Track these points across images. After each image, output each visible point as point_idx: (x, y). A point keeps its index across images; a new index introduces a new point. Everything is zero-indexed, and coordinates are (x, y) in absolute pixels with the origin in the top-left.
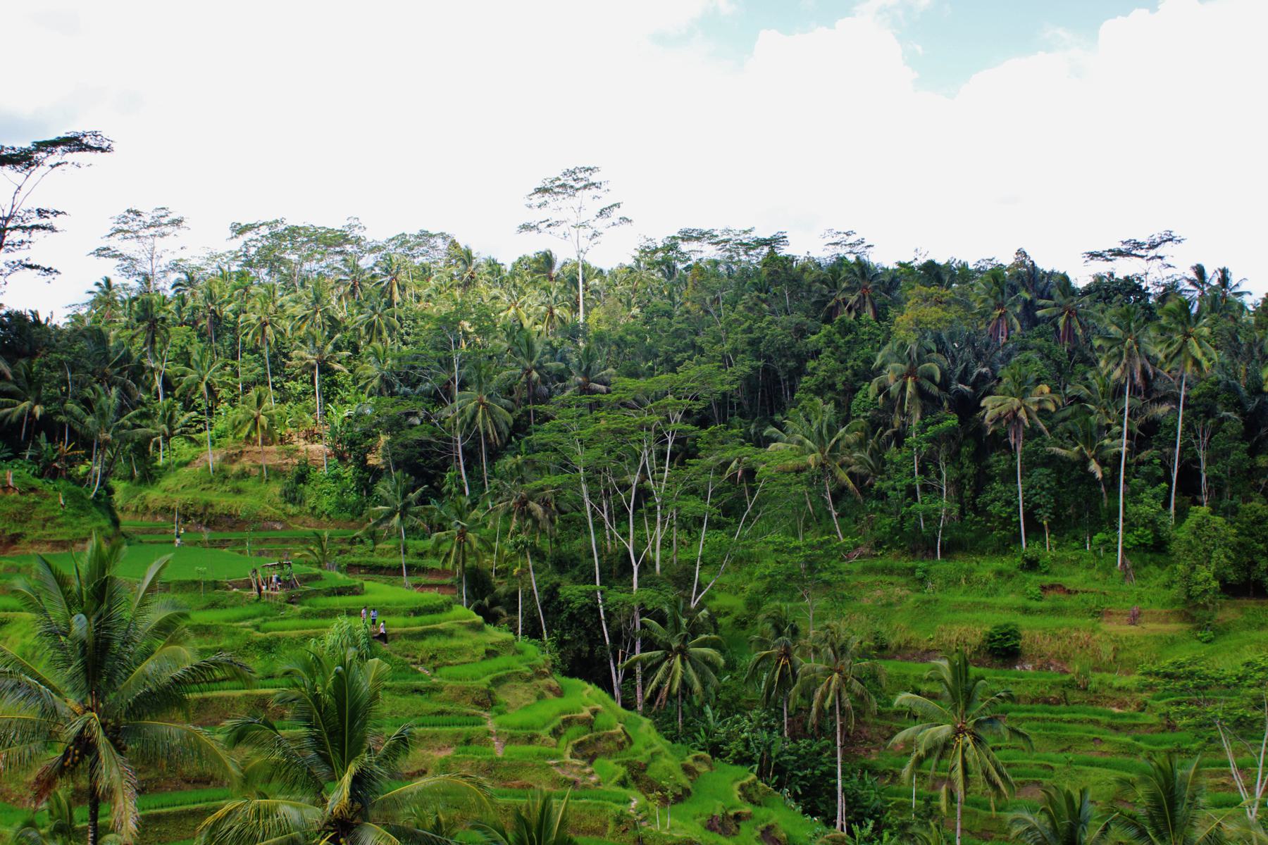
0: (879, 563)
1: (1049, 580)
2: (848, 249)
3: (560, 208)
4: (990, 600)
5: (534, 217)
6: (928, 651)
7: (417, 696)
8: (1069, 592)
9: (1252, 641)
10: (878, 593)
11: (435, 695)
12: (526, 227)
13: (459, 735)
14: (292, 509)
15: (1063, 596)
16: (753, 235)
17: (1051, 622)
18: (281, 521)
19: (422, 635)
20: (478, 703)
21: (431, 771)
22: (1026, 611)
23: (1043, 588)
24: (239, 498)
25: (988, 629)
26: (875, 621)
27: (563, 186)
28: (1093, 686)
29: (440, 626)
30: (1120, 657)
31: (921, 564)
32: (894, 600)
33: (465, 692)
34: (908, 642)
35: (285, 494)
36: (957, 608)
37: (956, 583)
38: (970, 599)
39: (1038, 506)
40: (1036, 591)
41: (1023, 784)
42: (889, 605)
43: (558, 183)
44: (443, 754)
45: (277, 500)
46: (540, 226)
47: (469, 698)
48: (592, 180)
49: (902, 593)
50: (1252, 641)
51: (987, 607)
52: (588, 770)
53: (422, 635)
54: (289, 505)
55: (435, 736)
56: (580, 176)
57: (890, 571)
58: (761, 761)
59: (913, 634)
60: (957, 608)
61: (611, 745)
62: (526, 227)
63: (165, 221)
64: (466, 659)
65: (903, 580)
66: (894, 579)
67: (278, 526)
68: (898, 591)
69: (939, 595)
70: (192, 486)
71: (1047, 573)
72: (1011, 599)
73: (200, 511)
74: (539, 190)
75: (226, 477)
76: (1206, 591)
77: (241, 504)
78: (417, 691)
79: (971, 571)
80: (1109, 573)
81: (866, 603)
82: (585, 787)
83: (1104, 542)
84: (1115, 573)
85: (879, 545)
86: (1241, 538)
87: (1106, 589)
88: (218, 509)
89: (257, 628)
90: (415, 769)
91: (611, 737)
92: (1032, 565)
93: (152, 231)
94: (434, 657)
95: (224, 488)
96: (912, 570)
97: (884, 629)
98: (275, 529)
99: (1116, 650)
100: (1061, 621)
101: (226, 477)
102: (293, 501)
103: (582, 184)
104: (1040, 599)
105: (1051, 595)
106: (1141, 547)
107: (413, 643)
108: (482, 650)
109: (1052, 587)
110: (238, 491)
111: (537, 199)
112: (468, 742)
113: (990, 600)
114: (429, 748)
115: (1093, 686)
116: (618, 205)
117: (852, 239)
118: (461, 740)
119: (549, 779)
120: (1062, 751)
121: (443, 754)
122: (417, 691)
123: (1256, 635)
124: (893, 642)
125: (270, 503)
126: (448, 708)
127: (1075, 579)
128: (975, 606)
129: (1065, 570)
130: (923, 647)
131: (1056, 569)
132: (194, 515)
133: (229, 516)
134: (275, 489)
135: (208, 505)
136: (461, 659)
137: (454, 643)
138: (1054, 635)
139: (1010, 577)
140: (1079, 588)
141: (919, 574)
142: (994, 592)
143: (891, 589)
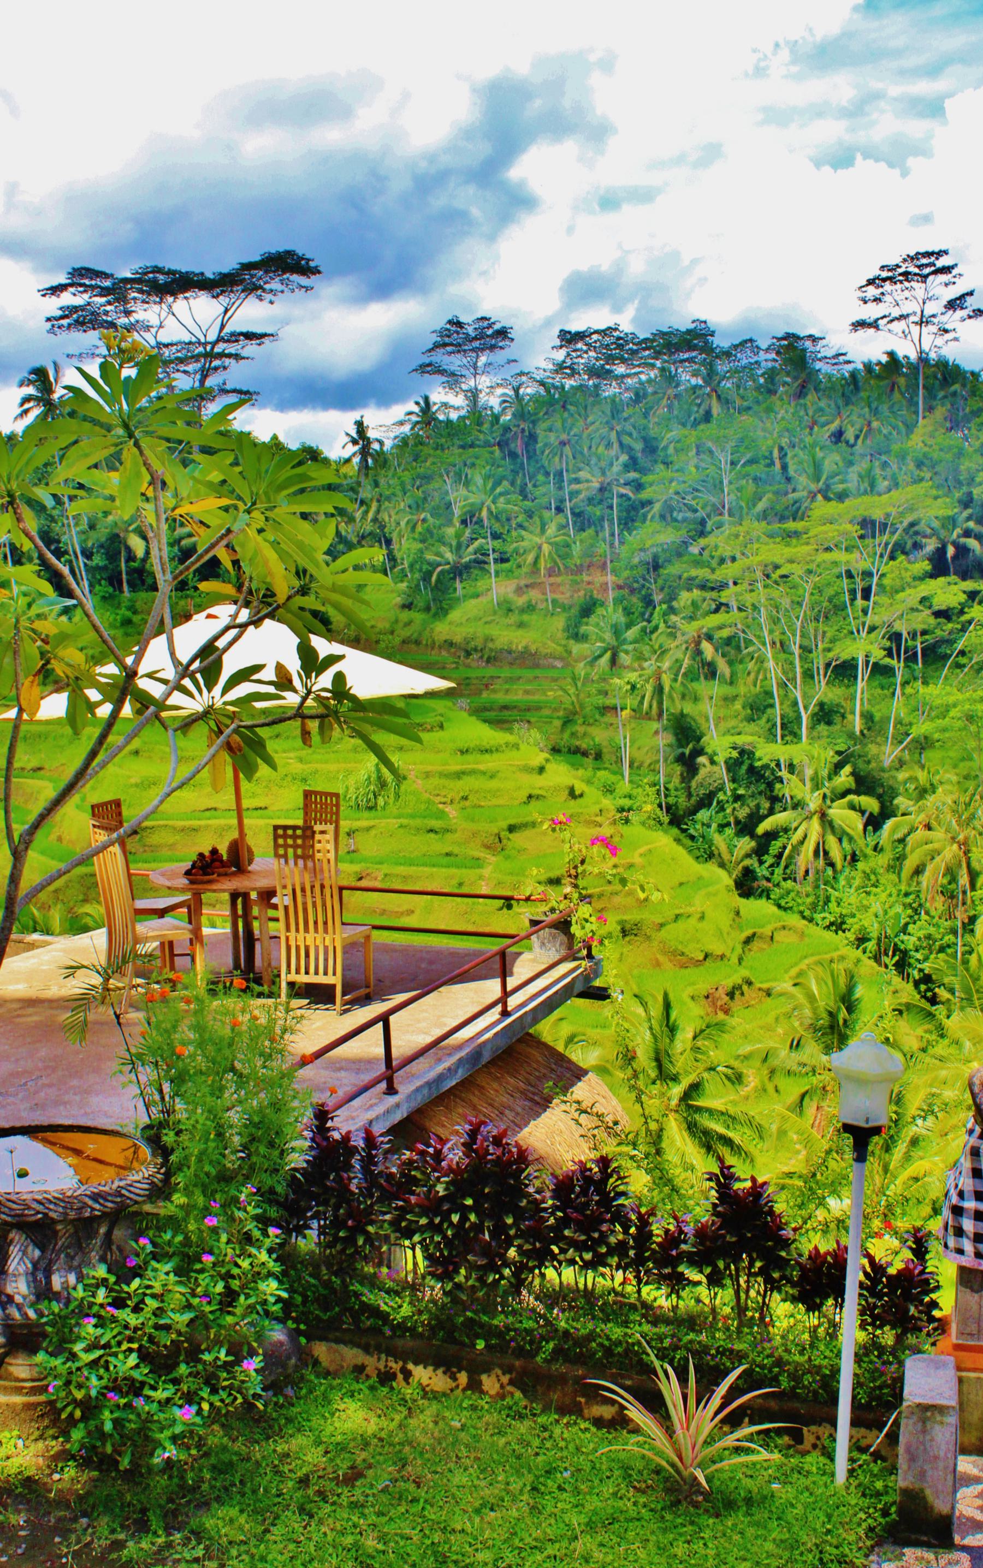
3: (905, 299)
5: (871, 312)
7: (432, 835)
11: (448, 836)
12: (860, 325)
13: (452, 877)
18: (561, 659)
19: (459, 775)
20: (487, 847)
21: (418, 912)
24: (520, 632)
29: (482, 767)
33: (474, 834)
35: (567, 629)
43: (900, 270)
45: (560, 635)
53: (459, 775)
54: (572, 642)
56: (924, 261)
58: (879, 939)
62: (860, 325)
63: (490, 332)
64: (501, 802)
67: (559, 664)
74: (871, 282)
75: (510, 610)
77: (519, 639)
88: (498, 644)
89: (301, 760)
93: (476, 344)
94: (465, 798)
98: (554, 667)
101: (510, 610)
108: (523, 795)
110: (521, 625)
111: (872, 291)
125: (552, 638)
126: (456, 850)
132: (476, 650)
134: (559, 623)
137: (493, 784)
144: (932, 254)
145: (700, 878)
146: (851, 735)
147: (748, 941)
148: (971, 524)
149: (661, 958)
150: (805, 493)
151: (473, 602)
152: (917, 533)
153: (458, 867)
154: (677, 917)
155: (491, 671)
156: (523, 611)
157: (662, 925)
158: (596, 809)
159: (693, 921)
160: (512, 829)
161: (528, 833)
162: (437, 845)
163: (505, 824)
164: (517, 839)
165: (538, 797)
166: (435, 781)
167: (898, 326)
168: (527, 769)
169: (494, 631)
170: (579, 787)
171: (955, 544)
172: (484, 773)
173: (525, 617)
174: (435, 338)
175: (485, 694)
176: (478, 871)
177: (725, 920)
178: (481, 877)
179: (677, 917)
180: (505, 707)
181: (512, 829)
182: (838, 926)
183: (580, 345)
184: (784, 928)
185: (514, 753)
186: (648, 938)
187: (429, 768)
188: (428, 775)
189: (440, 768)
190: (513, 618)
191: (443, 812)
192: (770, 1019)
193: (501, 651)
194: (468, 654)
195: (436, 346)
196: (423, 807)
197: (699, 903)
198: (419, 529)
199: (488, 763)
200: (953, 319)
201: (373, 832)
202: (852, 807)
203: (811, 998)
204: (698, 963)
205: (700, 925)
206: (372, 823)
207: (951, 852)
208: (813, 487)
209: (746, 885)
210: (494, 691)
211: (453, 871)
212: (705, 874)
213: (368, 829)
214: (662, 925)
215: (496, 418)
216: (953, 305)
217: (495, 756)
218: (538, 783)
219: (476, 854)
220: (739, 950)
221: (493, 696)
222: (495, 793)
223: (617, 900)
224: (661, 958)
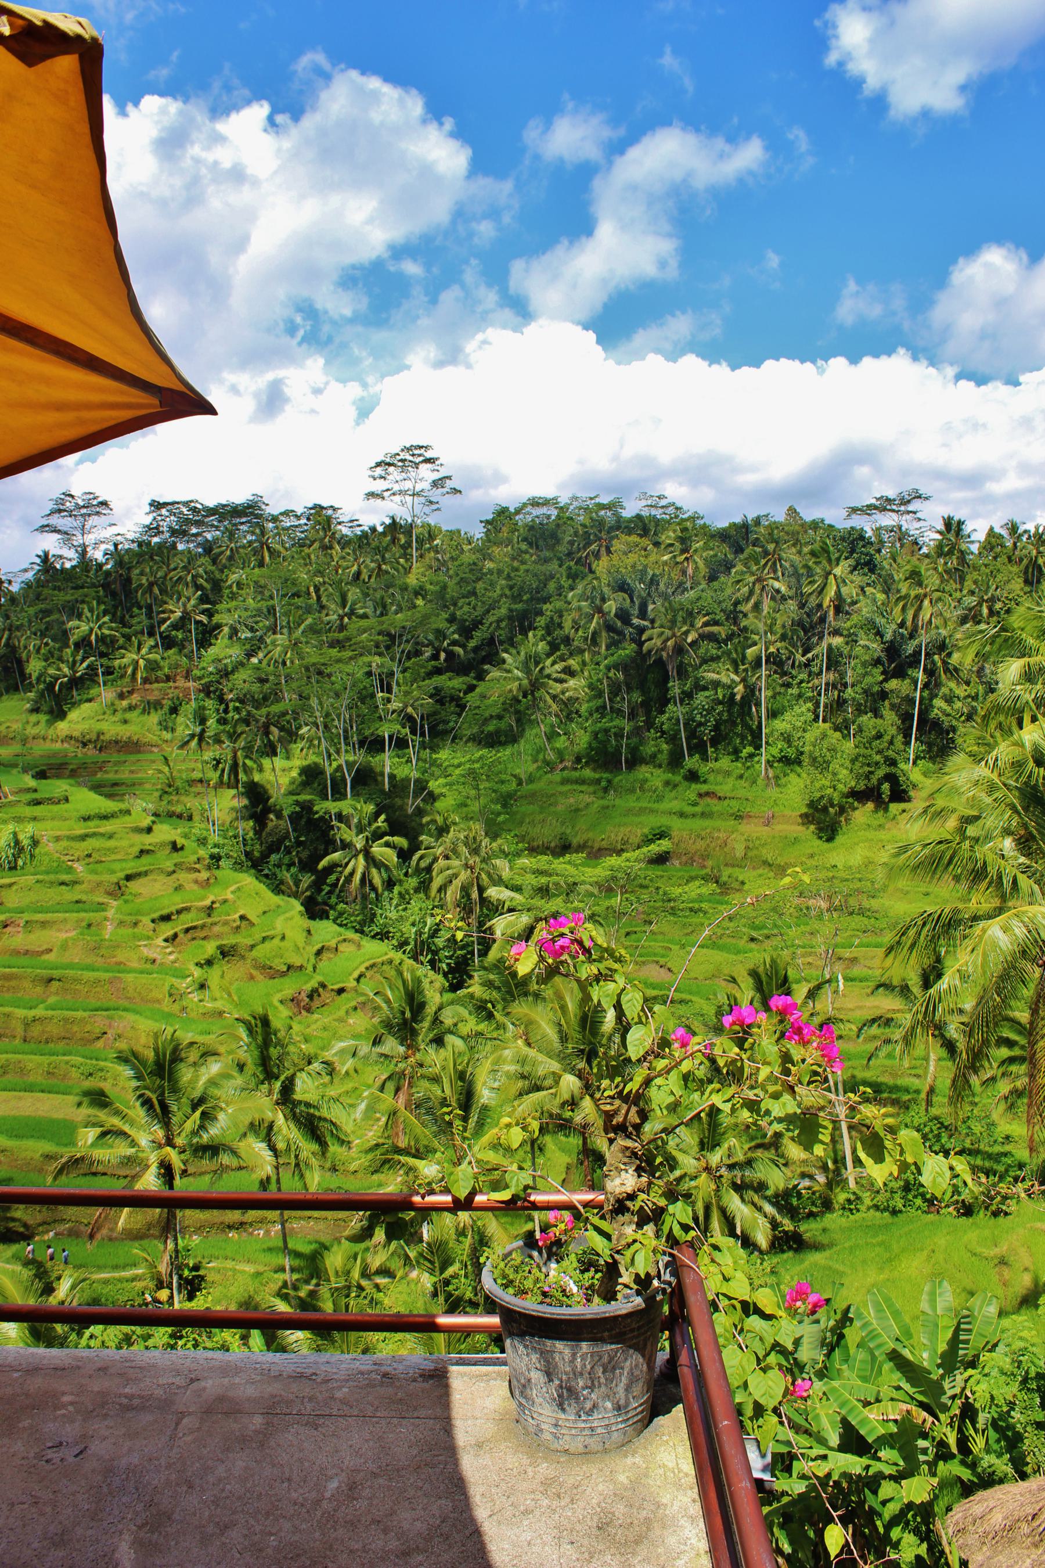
0: (576, 774)
1: (704, 788)
2: (661, 511)
4: (655, 806)
5: (379, 486)
6: (600, 849)
7: (64, 887)
8: (720, 798)
9: (867, 840)
10: (572, 800)
11: (77, 887)
13: (82, 920)
14: (167, 736)
15: (715, 801)
16: (597, 500)
17: (698, 824)
19: (83, 838)
20: (110, 894)
21: (55, 950)
22: (682, 815)
23: (700, 795)
24: (125, 727)
25: (646, 831)
26: (563, 823)
27: (401, 460)
28: (724, 878)
29: (102, 830)
30: (750, 854)
31: (605, 775)
32: (581, 806)
33: (99, 884)
34: (586, 842)
35: (160, 723)
36: (629, 812)
37: (632, 791)
38: (638, 805)
39: (700, 724)
40: (693, 797)
41: (644, 963)
42: (577, 810)
44: (63, 936)
45: (156, 728)
46: (386, 494)
47: (102, 890)
48: (429, 454)
49: (589, 800)
50: (867, 840)
51: (652, 811)
52: (168, 950)
53: (83, 838)
55: (65, 920)
56: (416, 452)
57: (582, 782)
59: (591, 835)
60: (629, 812)
61: (226, 929)
62: (371, 495)
63: (95, 502)
64: (119, 857)
65: (591, 789)
66: (583, 788)
68: (588, 799)
69: (618, 802)
70: (90, 718)
71: (705, 782)
72: (676, 805)
73: (94, 738)
74: (378, 465)
76: (822, 797)
78: (63, 883)
79: (646, 780)
80: (754, 782)
81: (560, 808)
82: (162, 964)
83: (751, 756)
84: (760, 782)
85: (578, 759)
86: (863, 751)
87: (750, 795)
88: (107, 737)
90: (45, 947)
91: (226, 923)
92: (693, 777)
94: (89, 856)
95: (114, 719)
96: (598, 781)
97: (568, 831)
99: (747, 848)
100: (707, 823)
102: (166, 728)
103: (421, 459)
104: (695, 804)
105: (708, 800)
106: (785, 760)
107: (73, 844)
108: (136, 850)
109: (707, 794)
110: (125, 722)
111: (379, 471)
112: (89, 926)
113: (655, 806)
114: (59, 930)
115: (724, 878)
116: (449, 478)
117: (663, 502)
118: (84, 924)
119: (136, 957)
120: (687, 934)
121: (63, 936)
122: (63, 883)
123: (871, 834)
124: (575, 841)
126: (84, 898)
127: (725, 787)
128: (642, 811)
129: (720, 778)
130: (596, 846)
131: (711, 778)
133: (117, 742)
135: (99, 734)
136: (113, 857)
137: (112, 843)
138: (698, 836)
139: (675, 786)
140: (728, 795)
141: (604, 784)
142: (660, 799)
143: (582, 795)
144: (421, 447)
145: (279, 907)
146: (383, 791)
147: (319, 953)
148: (456, 636)
149: (254, 972)
150: (335, 617)
151: (87, 705)
152: (417, 643)
153: (86, 911)
154: (264, 939)
155: (104, 757)
156: (125, 710)
157: (253, 946)
158: (194, 858)
159: (276, 941)
160: (128, 878)
161: (142, 881)
162: (69, 895)
163: (122, 875)
164: (134, 886)
165: (148, 852)
166: (64, 843)
167: (397, 498)
168: (139, 830)
169: (104, 726)
170: (180, 841)
171: (445, 650)
172: (102, 835)
173: (128, 716)
174: (51, 506)
175: (99, 775)
176: (103, 914)
177: (300, 938)
178: (106, 919)
179: (264, 939)
180: (115, 784)
181: (128, 878)
182: (383, 936)
183: (164, 512)
184: (345, 940)
185: (127, 818)
186: (243, 957)
187: (58, 833)
188: (58, 839)
189: (68, 833)
190: (119, 716)
191: (71, 867)
192: (342, 1013)
193: (110, 742)
194: (85, 745)
195: (52, 513)
196: (55, 864)
197: (280, 925)
198: (43, 651)
199: (107, 827)
200: (436, 494)
201: (15, 888)
202: (387, 845)
203: (388, 1001)
204: (283, 974)
205: (282, 944)
206: (13, 880)
207: (464, 876)
208: (341, 612)
209: (314, 910)
210: (106, 772)
211: (83, 915)
212: (282, 903)
213: (10, 885)
214: (253, 946)
215: (100, 566)
216: (435, 484)
217: (112, 821)
218: (147, 840)
219: (101, 900)
220: (313, 960)
221: (106, 776)
222: (113, 850)
223: (217, 929)
224: (254, 972)
